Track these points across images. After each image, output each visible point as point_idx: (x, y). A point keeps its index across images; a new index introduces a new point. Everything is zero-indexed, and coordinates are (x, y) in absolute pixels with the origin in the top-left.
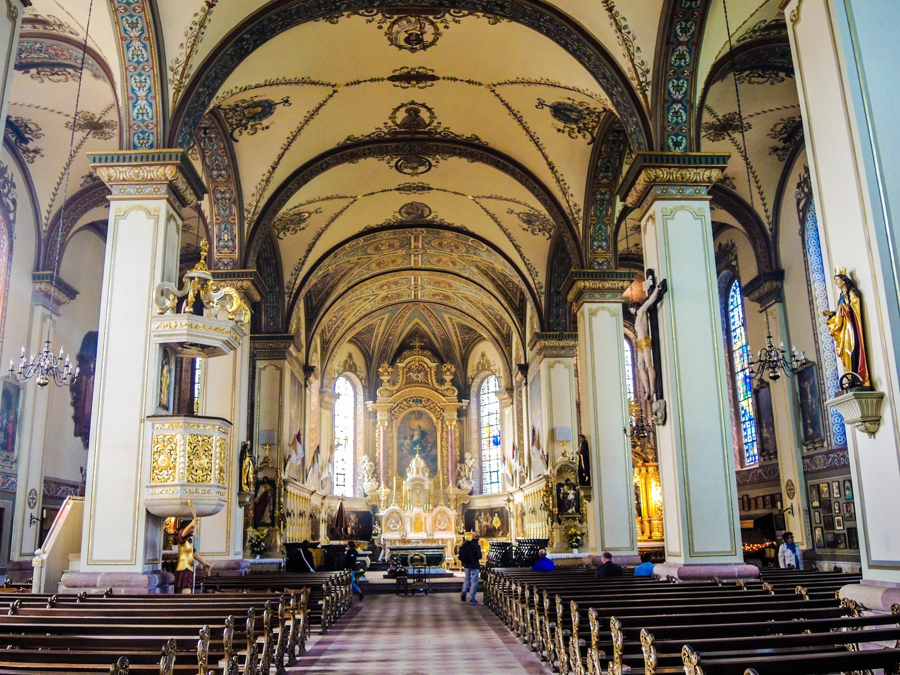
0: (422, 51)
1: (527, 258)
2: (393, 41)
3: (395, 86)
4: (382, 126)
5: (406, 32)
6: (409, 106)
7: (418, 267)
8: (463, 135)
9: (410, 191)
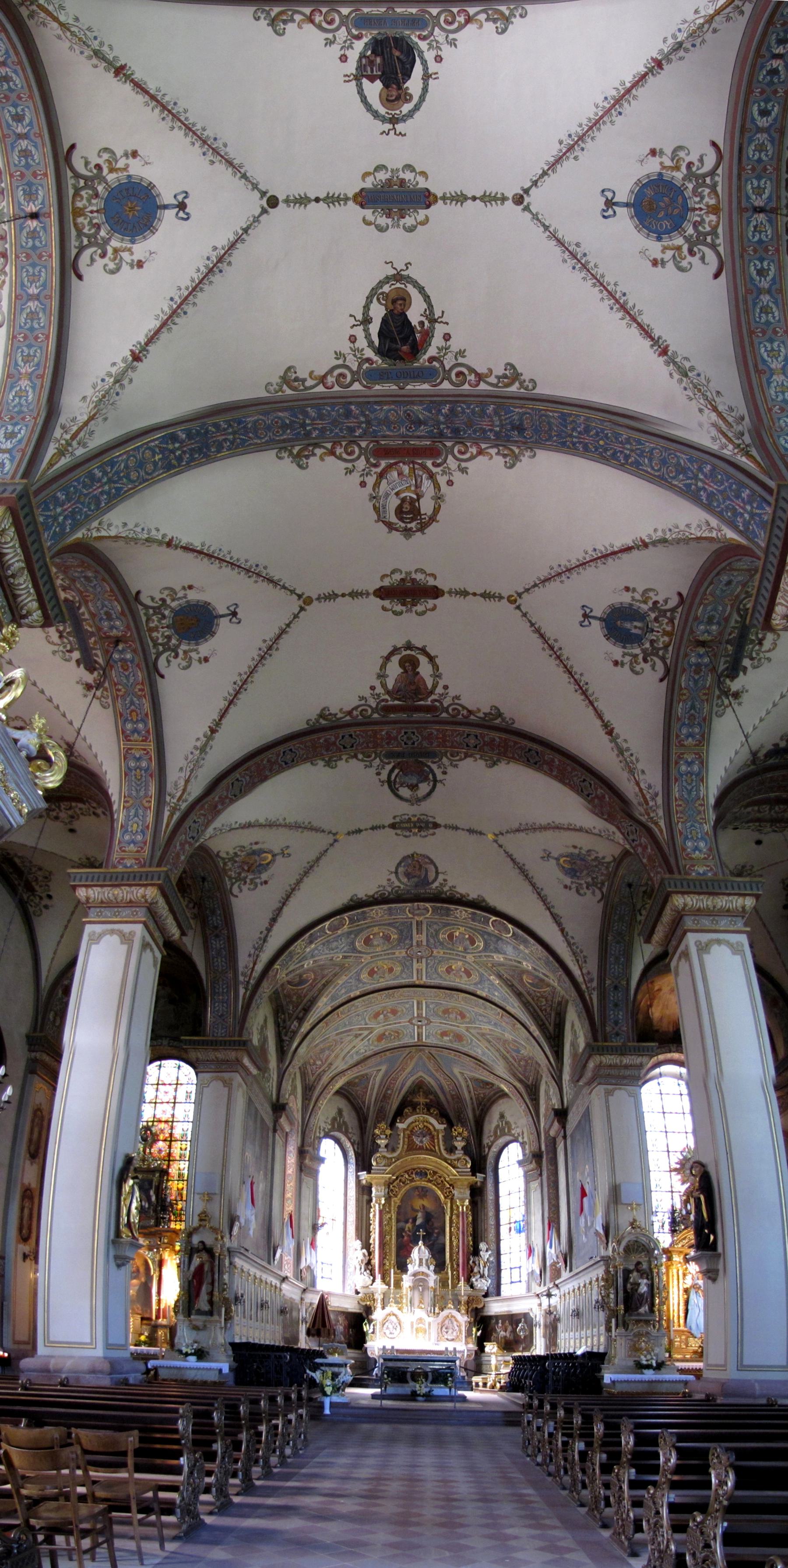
0: (419, 534)
1: (570, 934)
2: (381, 517)
3: (384, 609)
4: (367, 693)
5: (397, 494)
6: (404, 653)
7: (422, 983)
8: (479, 710)
9: (409, 829)
